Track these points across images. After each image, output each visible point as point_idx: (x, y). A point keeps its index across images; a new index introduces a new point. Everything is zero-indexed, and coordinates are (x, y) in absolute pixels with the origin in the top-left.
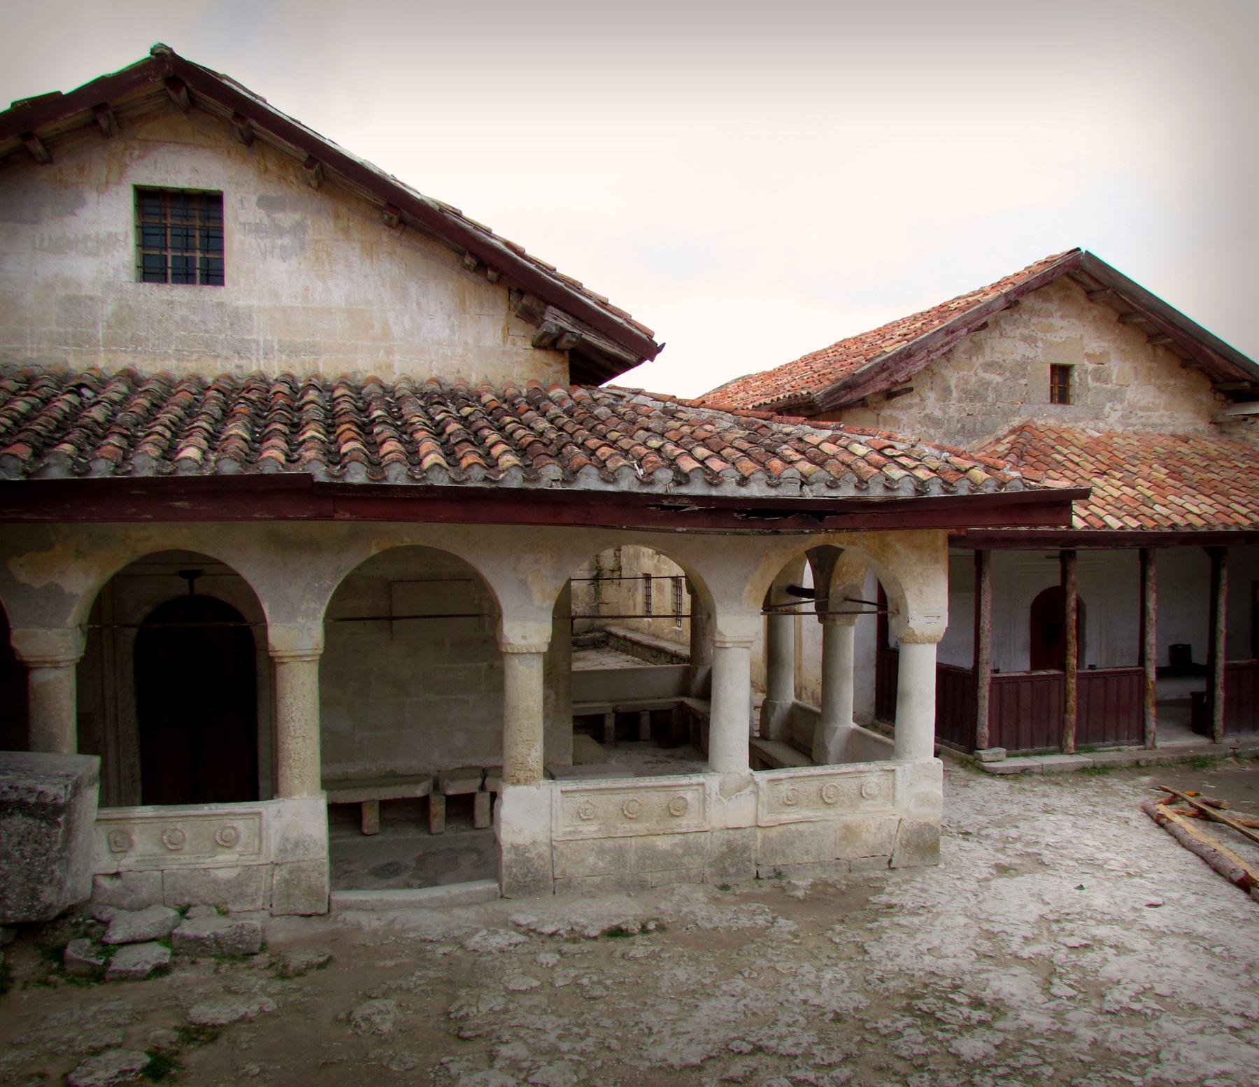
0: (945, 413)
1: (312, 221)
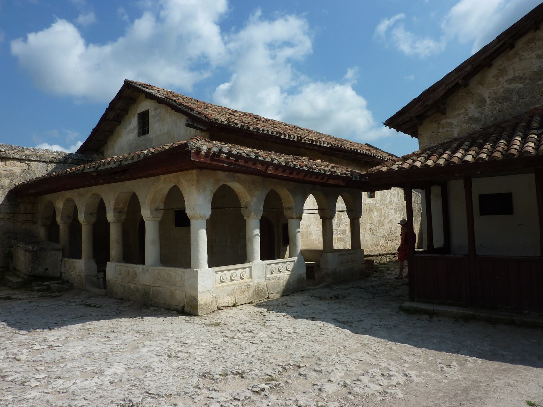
0: (482, 114)
1: (163, 110)
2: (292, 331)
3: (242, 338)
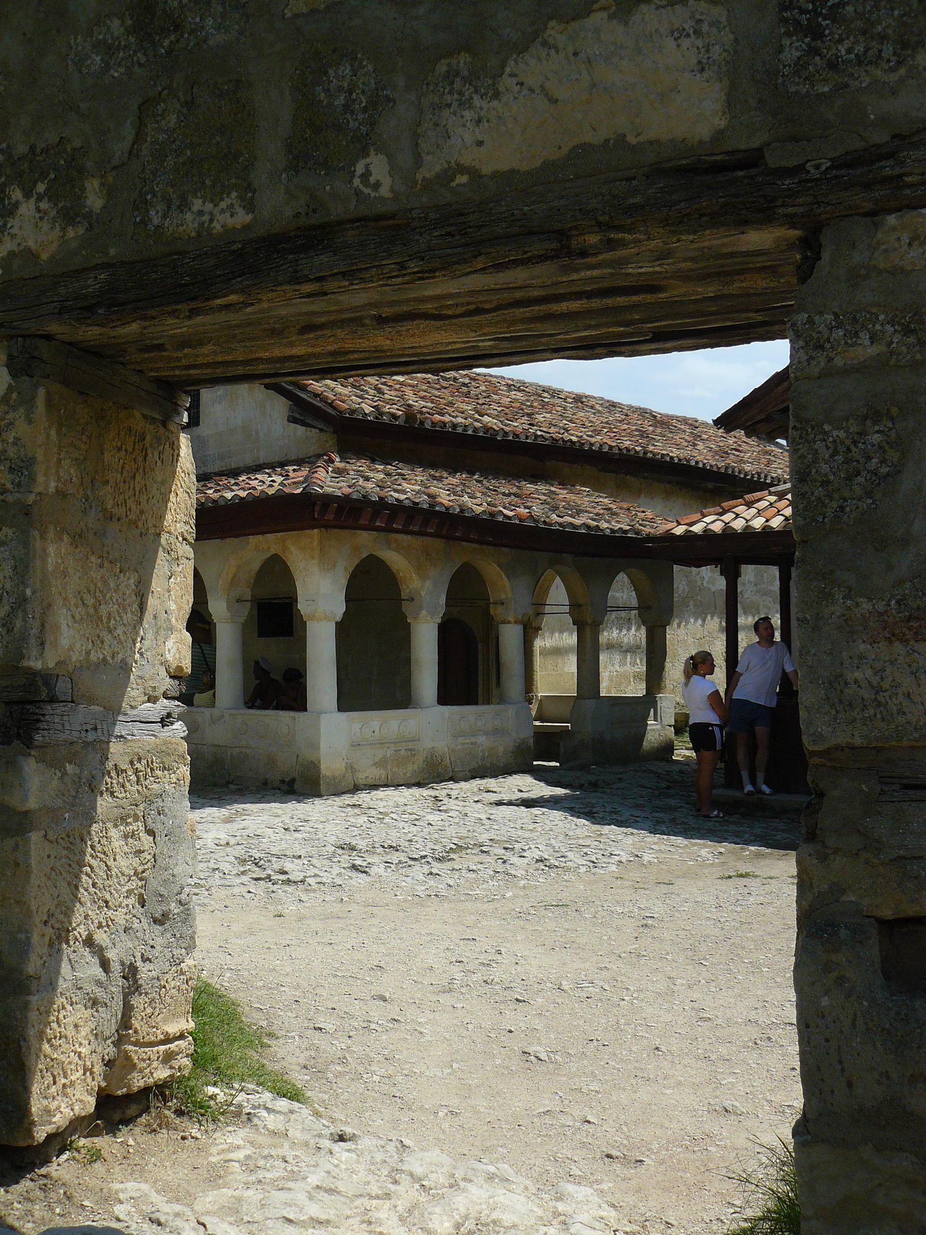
2: (483, 816)
3: (398, 819)
